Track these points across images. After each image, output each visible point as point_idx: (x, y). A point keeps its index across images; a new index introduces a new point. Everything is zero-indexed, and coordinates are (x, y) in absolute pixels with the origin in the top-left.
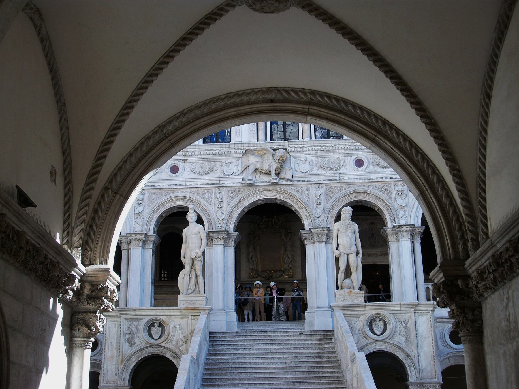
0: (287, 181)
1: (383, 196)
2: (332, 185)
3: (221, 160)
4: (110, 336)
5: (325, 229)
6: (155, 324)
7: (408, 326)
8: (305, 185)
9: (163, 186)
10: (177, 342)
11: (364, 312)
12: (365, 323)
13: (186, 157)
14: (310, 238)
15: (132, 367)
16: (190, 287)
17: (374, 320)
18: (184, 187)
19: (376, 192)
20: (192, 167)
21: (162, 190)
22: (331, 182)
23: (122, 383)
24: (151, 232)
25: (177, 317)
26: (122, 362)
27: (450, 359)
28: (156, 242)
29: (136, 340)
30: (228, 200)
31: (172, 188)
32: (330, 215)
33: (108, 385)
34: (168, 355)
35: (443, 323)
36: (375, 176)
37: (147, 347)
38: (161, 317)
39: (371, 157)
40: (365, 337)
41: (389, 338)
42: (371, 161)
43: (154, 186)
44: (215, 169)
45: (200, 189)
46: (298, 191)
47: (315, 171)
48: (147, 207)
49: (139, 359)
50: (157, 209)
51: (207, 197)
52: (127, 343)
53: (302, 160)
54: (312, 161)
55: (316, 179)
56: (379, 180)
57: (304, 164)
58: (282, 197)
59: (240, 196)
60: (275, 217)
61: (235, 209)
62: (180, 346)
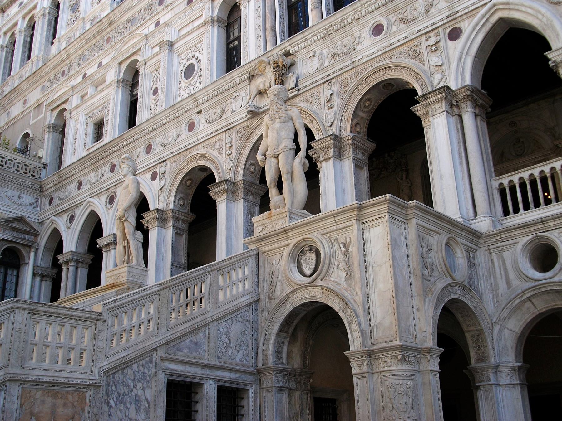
0: (292, 92)
2: (346, 75)
5: (329, 138)
7: (350, 250)
11: (286, 243)
13: (199, 108)
17: (303, 252)
22: (343, 71)
27: (533, 300)
28: (182, 217)
32: (345, 117)
35: (512, 237)
36: (397, 39)
41: (320, 277)
43: (172, 153)
44: (226, 110)
45: (212, 139)
47: (326, 64)
51: (218, 147)
56: (403, 42)
60: (386, 155)
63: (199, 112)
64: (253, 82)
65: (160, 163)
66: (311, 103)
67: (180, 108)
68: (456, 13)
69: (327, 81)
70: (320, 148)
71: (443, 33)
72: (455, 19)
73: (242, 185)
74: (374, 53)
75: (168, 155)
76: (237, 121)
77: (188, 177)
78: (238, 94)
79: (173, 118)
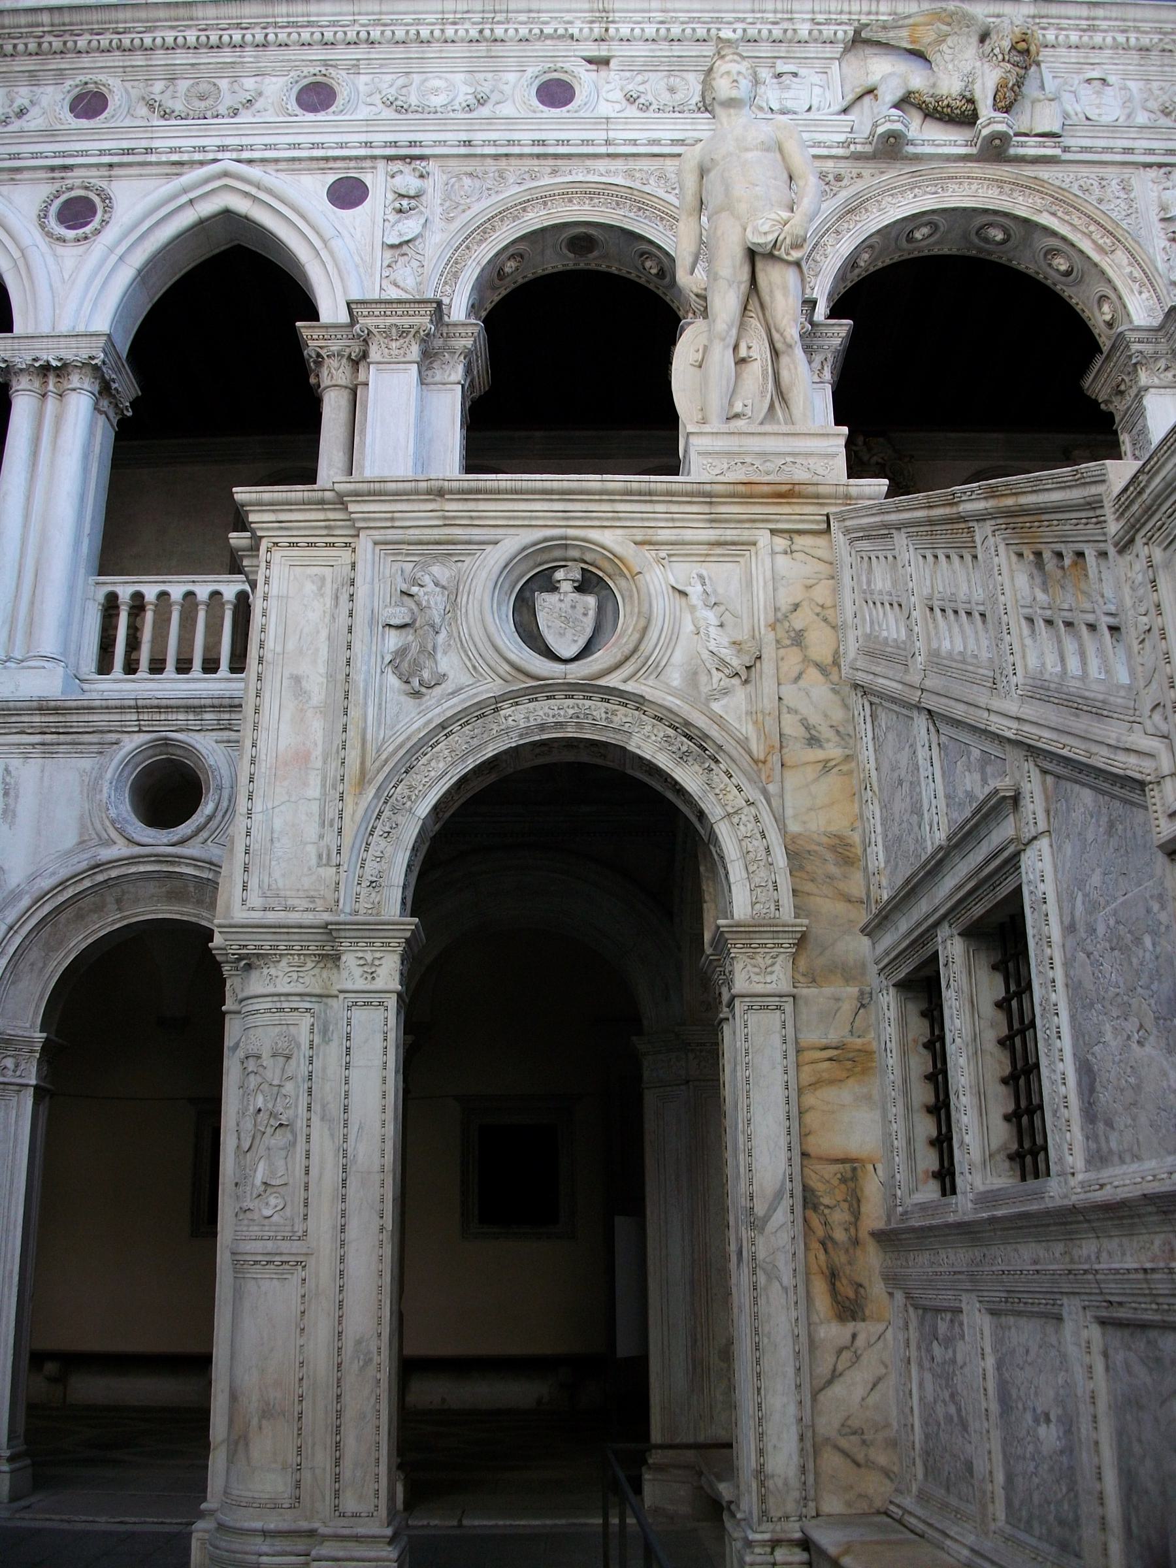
4: (291, 646)
6: (559, 575)
8: (1110, 169)
9: (511, 143)
10: (695, 673)
14: (1162, 364)
15: (424, 808)
16: (738, 407)
18: (603, 150)
20: (630, 87)
21: (503, 162)
23: (363, 906)
24: (458, 310)
25: (689, 535)
26: (363, 779)
29: (448, 663)
31: (545, 156)
33: (271, 917)
34: (648, 744)
37: (514, 698)
38: (594, 535)
43: (468, 143)
48: (437, 223)
49: (470, 763)
50: (484, 230)
52: (393, 680)
53: (1089, 81)
55: (1155, 145)
58: (1022, 206)
59: (844, 195)
61: (829, 239)
62: (713, 697)
63: (602, 62)
64: (850, 57)
65: (389, 158)
66: (1100, 201)
67: (523, 17)
69: (1160, 165)
77: (521, 247)
78: (791, 68)
79: (474, 33)
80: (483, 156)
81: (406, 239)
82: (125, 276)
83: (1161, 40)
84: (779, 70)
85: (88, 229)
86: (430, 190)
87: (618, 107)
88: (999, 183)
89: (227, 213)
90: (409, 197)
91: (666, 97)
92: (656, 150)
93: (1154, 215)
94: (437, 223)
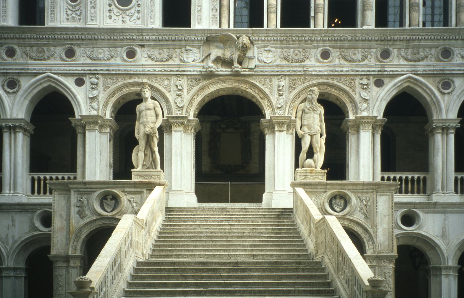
0: (249, 71)
1: (348, 89)
2: (296, 78)
3: (180, 47)
7: (369, 204)
9: (119, 70)
12: (326, 200)
18: (142, 73)
19: (341, 85)
21: (118, 75)
22: (295, 73)
30: (188, 88)
39: (338, 50)
40: (324, 213)
41: (349, 214)
42: (338, 54)
43: (108, 70)
44: (174, 55)
45: (158, 76)
46: (260, 82)
47: (278, 62)
50: (112, 94)
51: (166, 84)
53: (266, 51)
54: (277, 52)
57: (268, 54)
58: (244, 87)
59: (201, 85)
61: (195, 97)
63: (143, 46)
65: (89, 74)
66: (263, 85)
68: (385, 71)
69: (280, 75)
70: (277, 122)
71: (372, 80)
72: (382, 74)
73: (194, 123)
74: (322, 71)
75: (102, 70)
76: (190, 71)
78: (190, 48)
80: (112, 74)
81: (94, 96)
82: (27, 102)
83: (286, 38)
84: (187, 49)
85: (15, 90)
86: (100, 83)
87: (146, 59)
88: (238, 81)
89: (50, 86)
90: (95, 85)
91: (158, 56)
92: (155, 73)
93: (276, 89)
94: (102, 91)
